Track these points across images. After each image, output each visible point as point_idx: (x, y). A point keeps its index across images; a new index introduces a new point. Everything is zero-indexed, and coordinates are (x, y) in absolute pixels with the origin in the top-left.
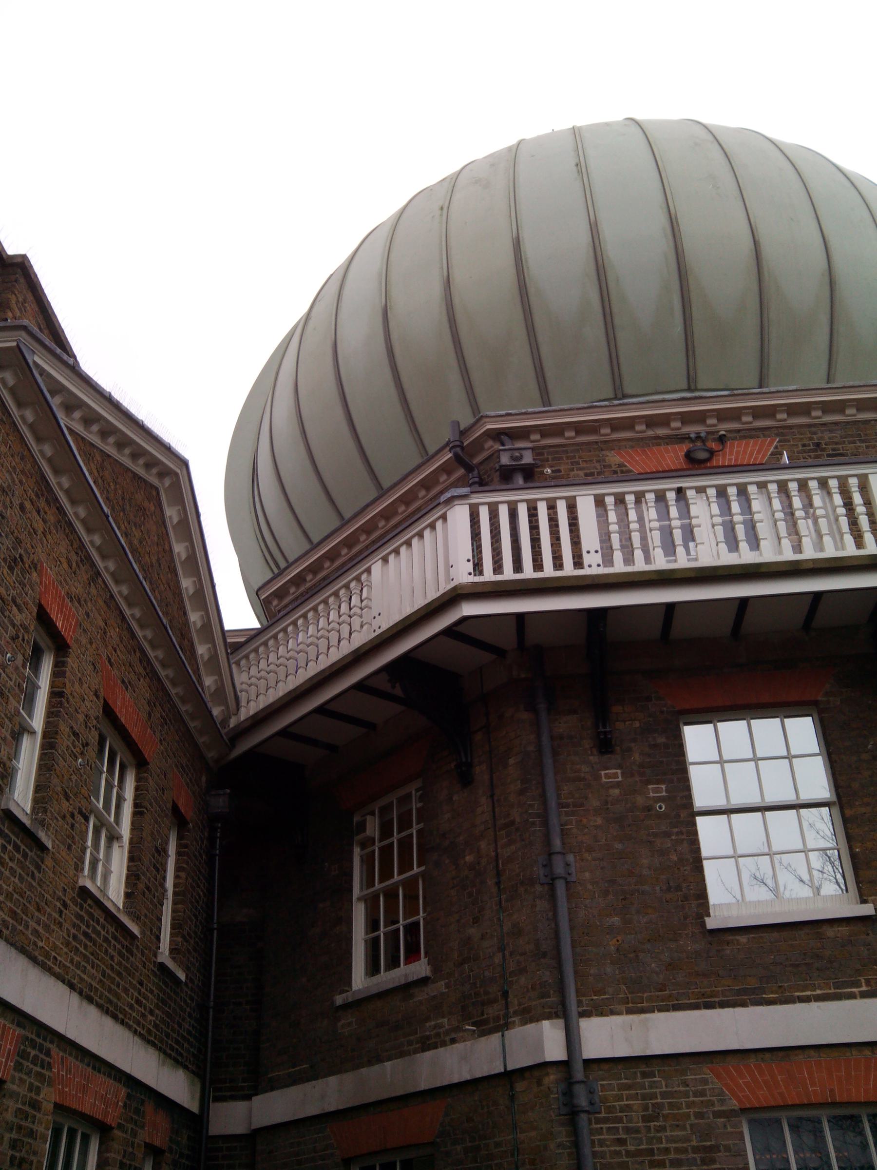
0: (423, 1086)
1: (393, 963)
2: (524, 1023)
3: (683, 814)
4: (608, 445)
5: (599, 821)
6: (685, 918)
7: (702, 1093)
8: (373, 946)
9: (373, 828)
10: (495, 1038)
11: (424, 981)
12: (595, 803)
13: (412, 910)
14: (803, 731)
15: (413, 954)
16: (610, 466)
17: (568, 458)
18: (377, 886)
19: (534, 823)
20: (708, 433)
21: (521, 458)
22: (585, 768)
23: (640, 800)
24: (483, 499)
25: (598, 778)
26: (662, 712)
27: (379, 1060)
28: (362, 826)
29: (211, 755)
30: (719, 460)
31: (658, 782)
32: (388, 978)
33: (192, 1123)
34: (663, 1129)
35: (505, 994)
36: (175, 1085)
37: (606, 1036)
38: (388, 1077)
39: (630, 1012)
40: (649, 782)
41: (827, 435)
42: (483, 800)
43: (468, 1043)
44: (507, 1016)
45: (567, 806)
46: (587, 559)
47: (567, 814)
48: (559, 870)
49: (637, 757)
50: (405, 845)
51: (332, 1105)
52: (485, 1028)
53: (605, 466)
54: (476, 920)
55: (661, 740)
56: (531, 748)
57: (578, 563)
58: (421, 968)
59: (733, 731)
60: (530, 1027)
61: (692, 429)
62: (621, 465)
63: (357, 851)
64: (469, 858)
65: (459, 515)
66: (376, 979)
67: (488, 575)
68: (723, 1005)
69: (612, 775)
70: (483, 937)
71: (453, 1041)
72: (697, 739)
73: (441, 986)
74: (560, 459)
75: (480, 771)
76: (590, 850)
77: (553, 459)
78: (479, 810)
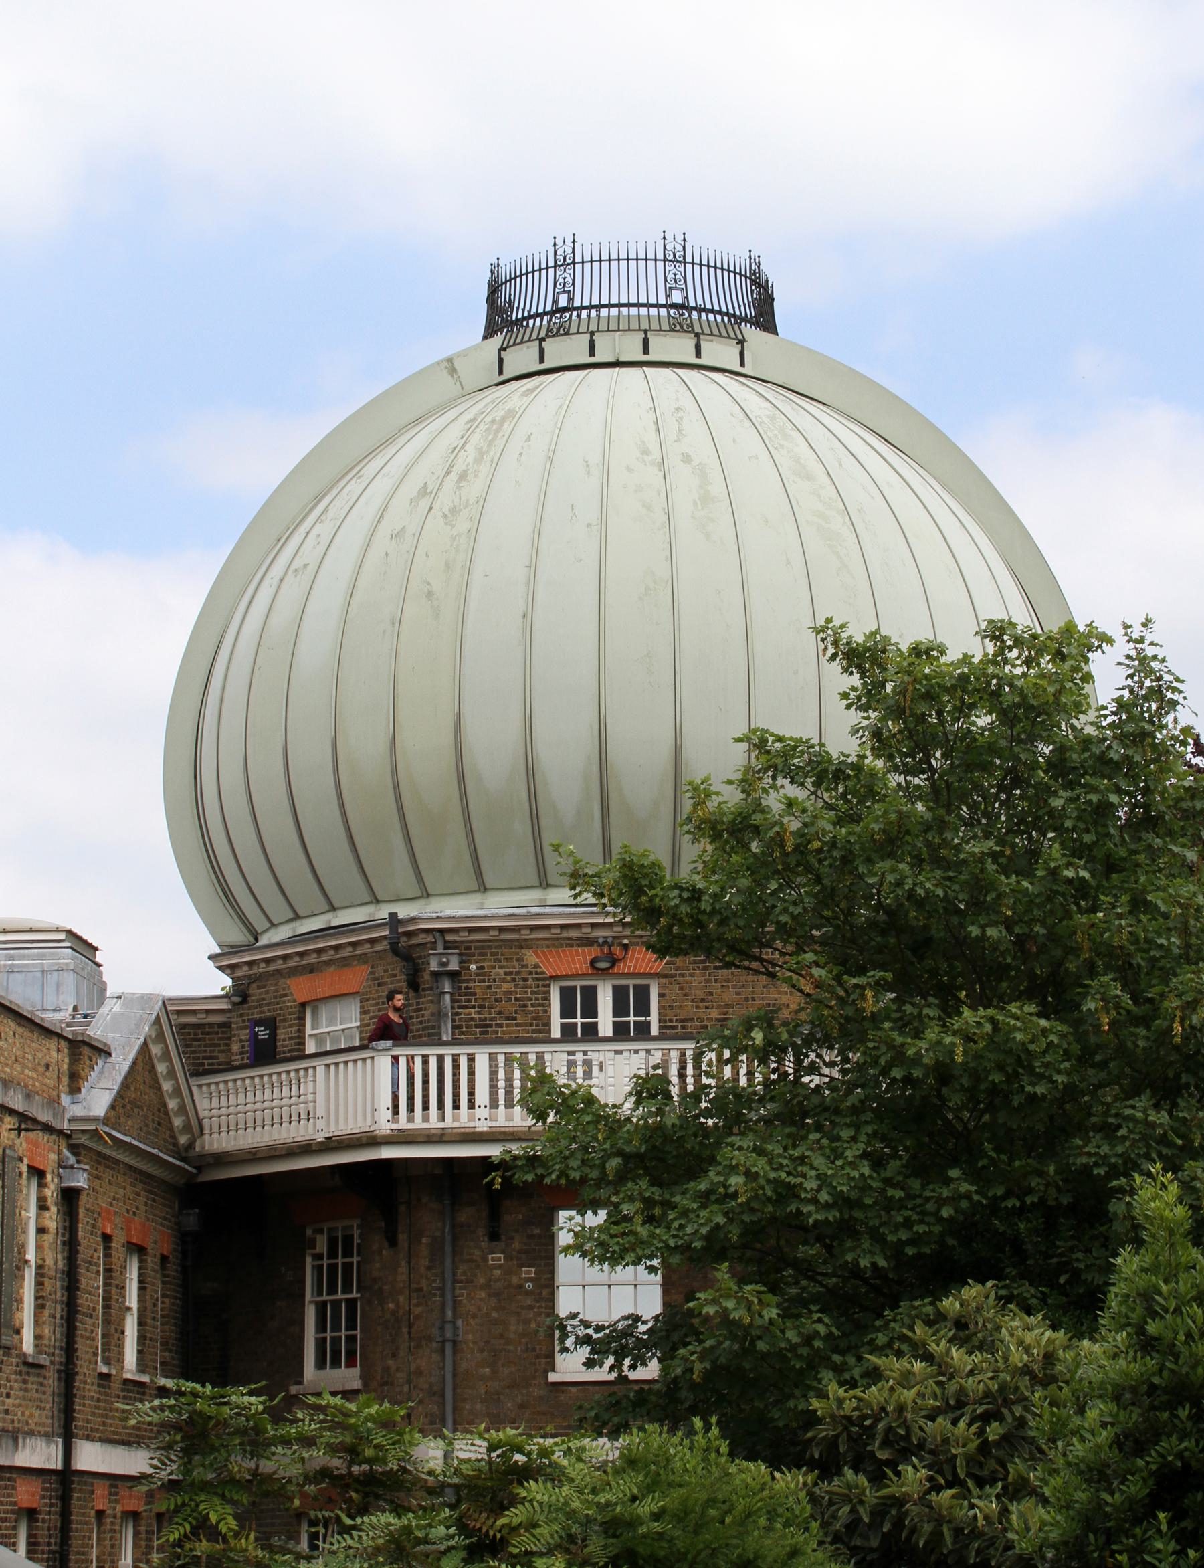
1: (336, 1363)
3: (545, 1292)
6: (536, 1371)
9: (322, 1245)
12: (482, 1281)
13: (351, 1325)
15: (351, 1363)
16: (527, 966)
17: (492, 954)
19: (435, 1295)
20: (614, 937)
22: (477, 1252)
23: (515, 1280)
24: (402, 1052)
25: (485, 1260)
26: (540, 1208)
30: (621, 968)
40: (523, 1265)
42: (403, 1263)
45: (461, 1282)
47: (461, 1288)
49: (517, 1245)
50: (348, 1267)
53: (523, 966)
54: (394, 1355)
55: (537, 1231)
56: (438, 1234)
62: (536, 966)
63: (309, 1260)
64: (391, 1306)
65: (383, 1063)
67: (403, 1123)
70: (398, 1369)
74: (486, 954)
75: (402, 1237)
76: (474, 1317)
77: (480, 954)
78: (400, 1270)
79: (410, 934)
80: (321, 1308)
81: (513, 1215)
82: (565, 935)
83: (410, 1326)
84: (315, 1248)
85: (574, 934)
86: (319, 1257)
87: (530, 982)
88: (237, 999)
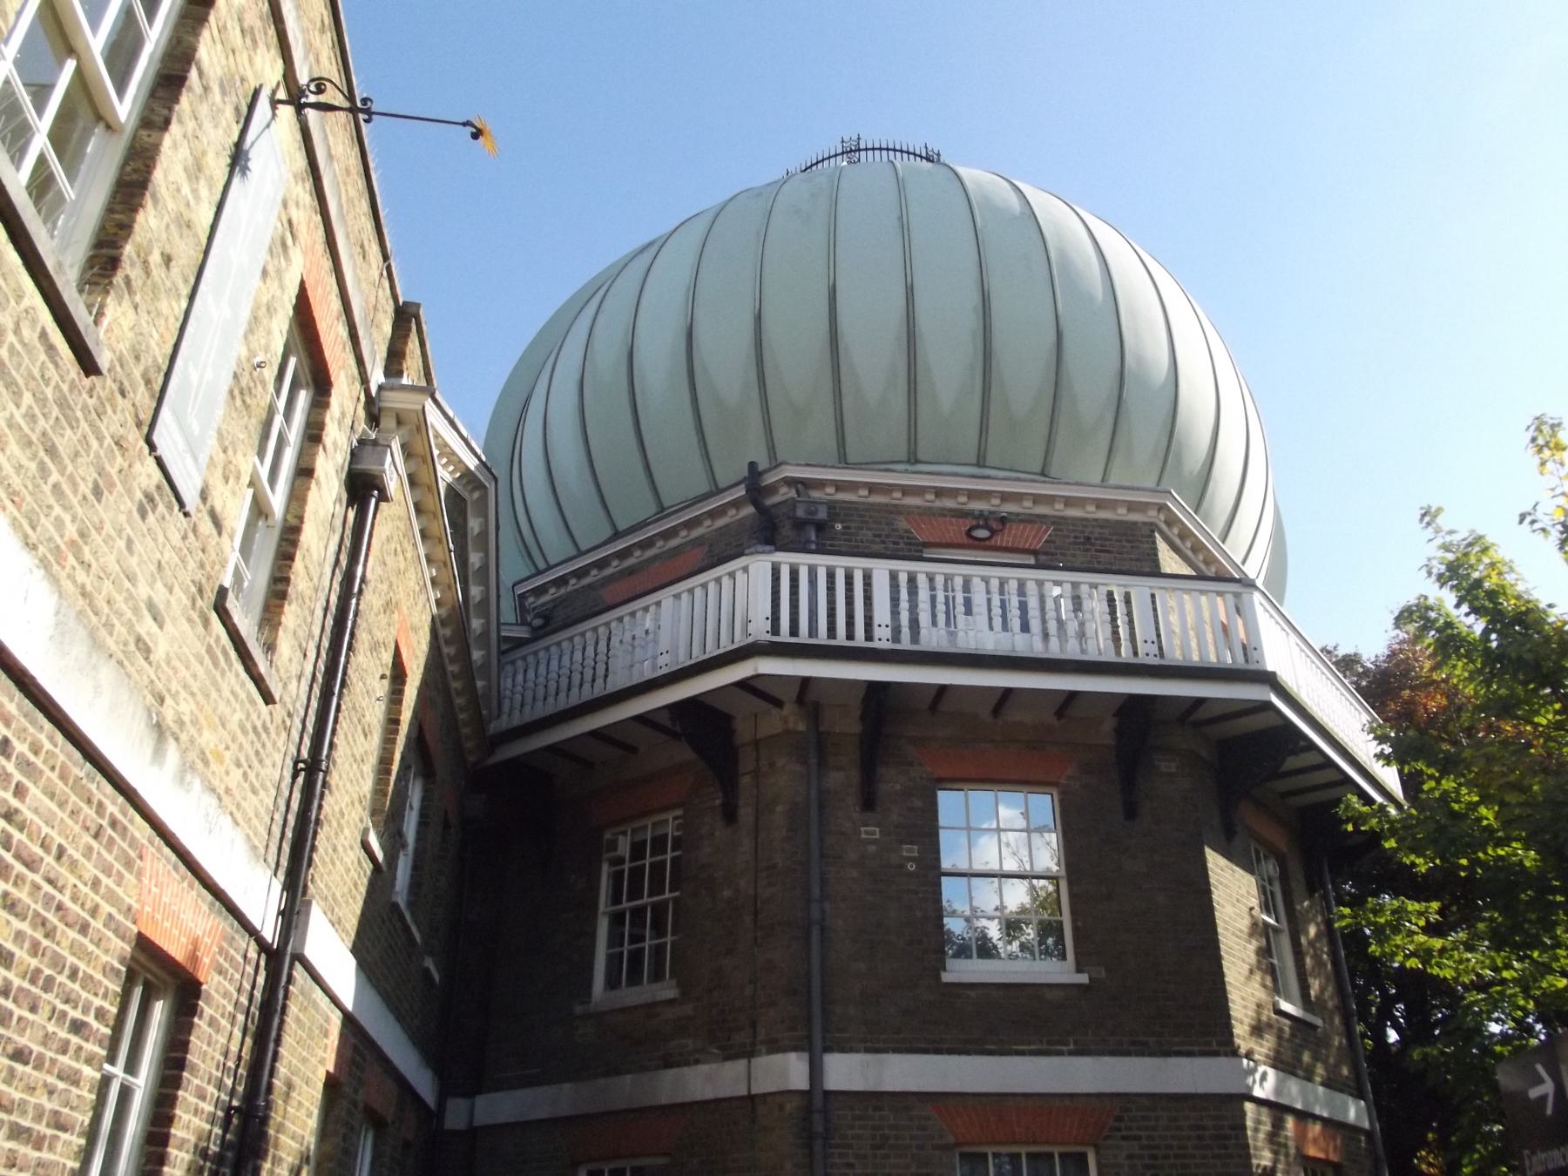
0: (664, 1100)
1: (635, 978)
2: (771, 1051)
4: (896, 510)
5: (855, 874)
7: (924, 1128)
8: (614, 961)
9: (624, 847)
10: (742, 1063)
11: (671, 1002)
12: (853, 856)
13: (659, 930)
14: (1043, 805)
15: (657, 976)
18: (625, 905)
21: (816, 512)
27: (618, 1072)
28: (613, 845)
29: (471, 759)
30: (998, 540)
31: (912, 843)
32: (631, 996)
33: (431, 1117)
34: (886, 1157)
35: (754, 1025)
36: (423, 1082)
37: (846, 1071)
38: (626, 1090)
39: (867, 1051)
40: (902, 842)
41: (1097, 530)
43: (714, 1066)
44: (753, 1044)
46: (877, 633)
48: (815, 914)
51: (564, 1110)
52: (730, 1054)
55: (918, 803)
57: (869, 637)
58: (667, 990)
59: (980, 798)
60: (777, 1058)
61: (977, 506)
62: (907, 531)
63: (605, 868)
64: (727, 893)
66: (616, 993)
68: (950, 1052)
69: (871, 832)
71: (697, 1062)
72: (949, 803)
73: (688, 1009)
75: (745, 813)
79: (772, 490)
80: (617, 919)
81: (892, 782)
82: (938, 504)
83: (756, 913)
84: (615, 849)
85: (949, 503)
86: (621, 861)
87: (902, 545)
88: (538, 622)
